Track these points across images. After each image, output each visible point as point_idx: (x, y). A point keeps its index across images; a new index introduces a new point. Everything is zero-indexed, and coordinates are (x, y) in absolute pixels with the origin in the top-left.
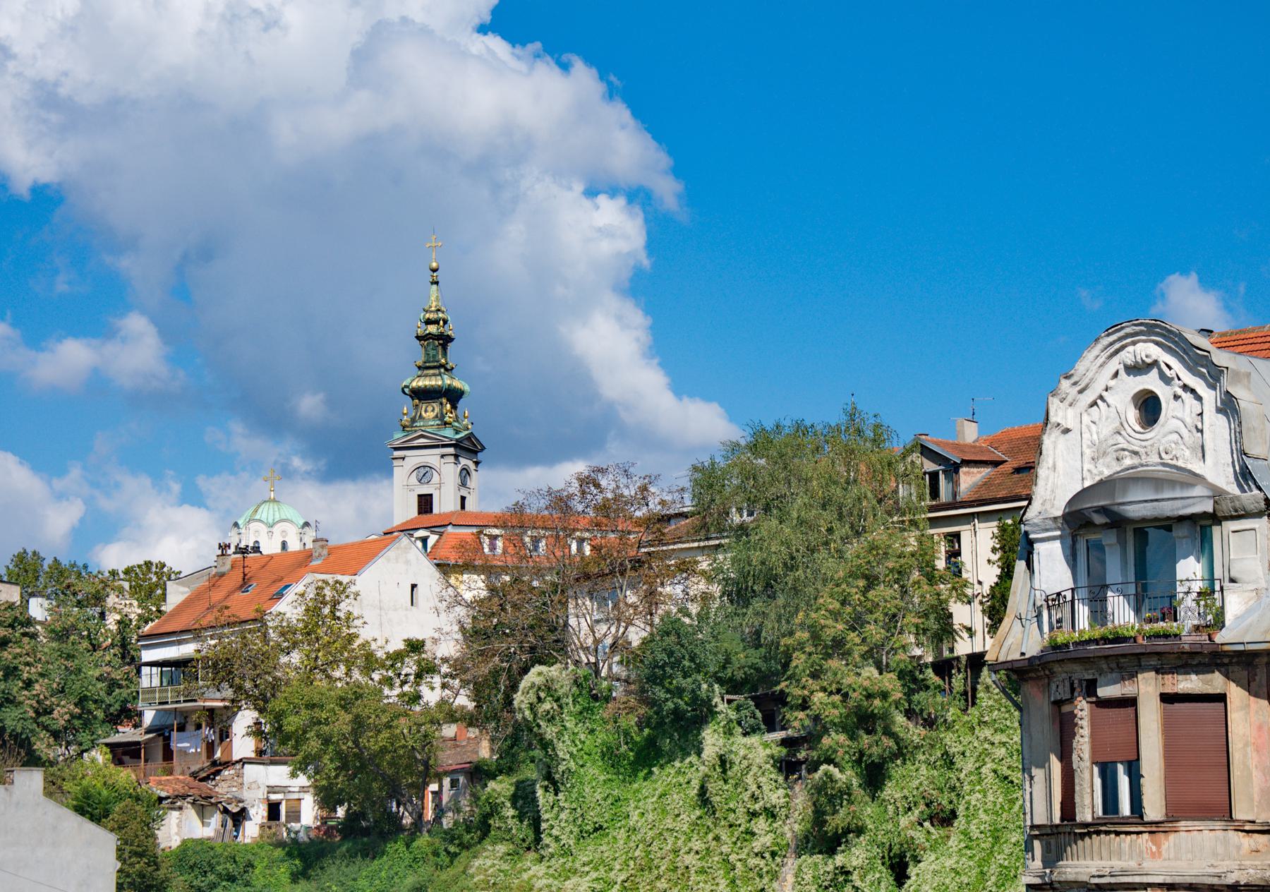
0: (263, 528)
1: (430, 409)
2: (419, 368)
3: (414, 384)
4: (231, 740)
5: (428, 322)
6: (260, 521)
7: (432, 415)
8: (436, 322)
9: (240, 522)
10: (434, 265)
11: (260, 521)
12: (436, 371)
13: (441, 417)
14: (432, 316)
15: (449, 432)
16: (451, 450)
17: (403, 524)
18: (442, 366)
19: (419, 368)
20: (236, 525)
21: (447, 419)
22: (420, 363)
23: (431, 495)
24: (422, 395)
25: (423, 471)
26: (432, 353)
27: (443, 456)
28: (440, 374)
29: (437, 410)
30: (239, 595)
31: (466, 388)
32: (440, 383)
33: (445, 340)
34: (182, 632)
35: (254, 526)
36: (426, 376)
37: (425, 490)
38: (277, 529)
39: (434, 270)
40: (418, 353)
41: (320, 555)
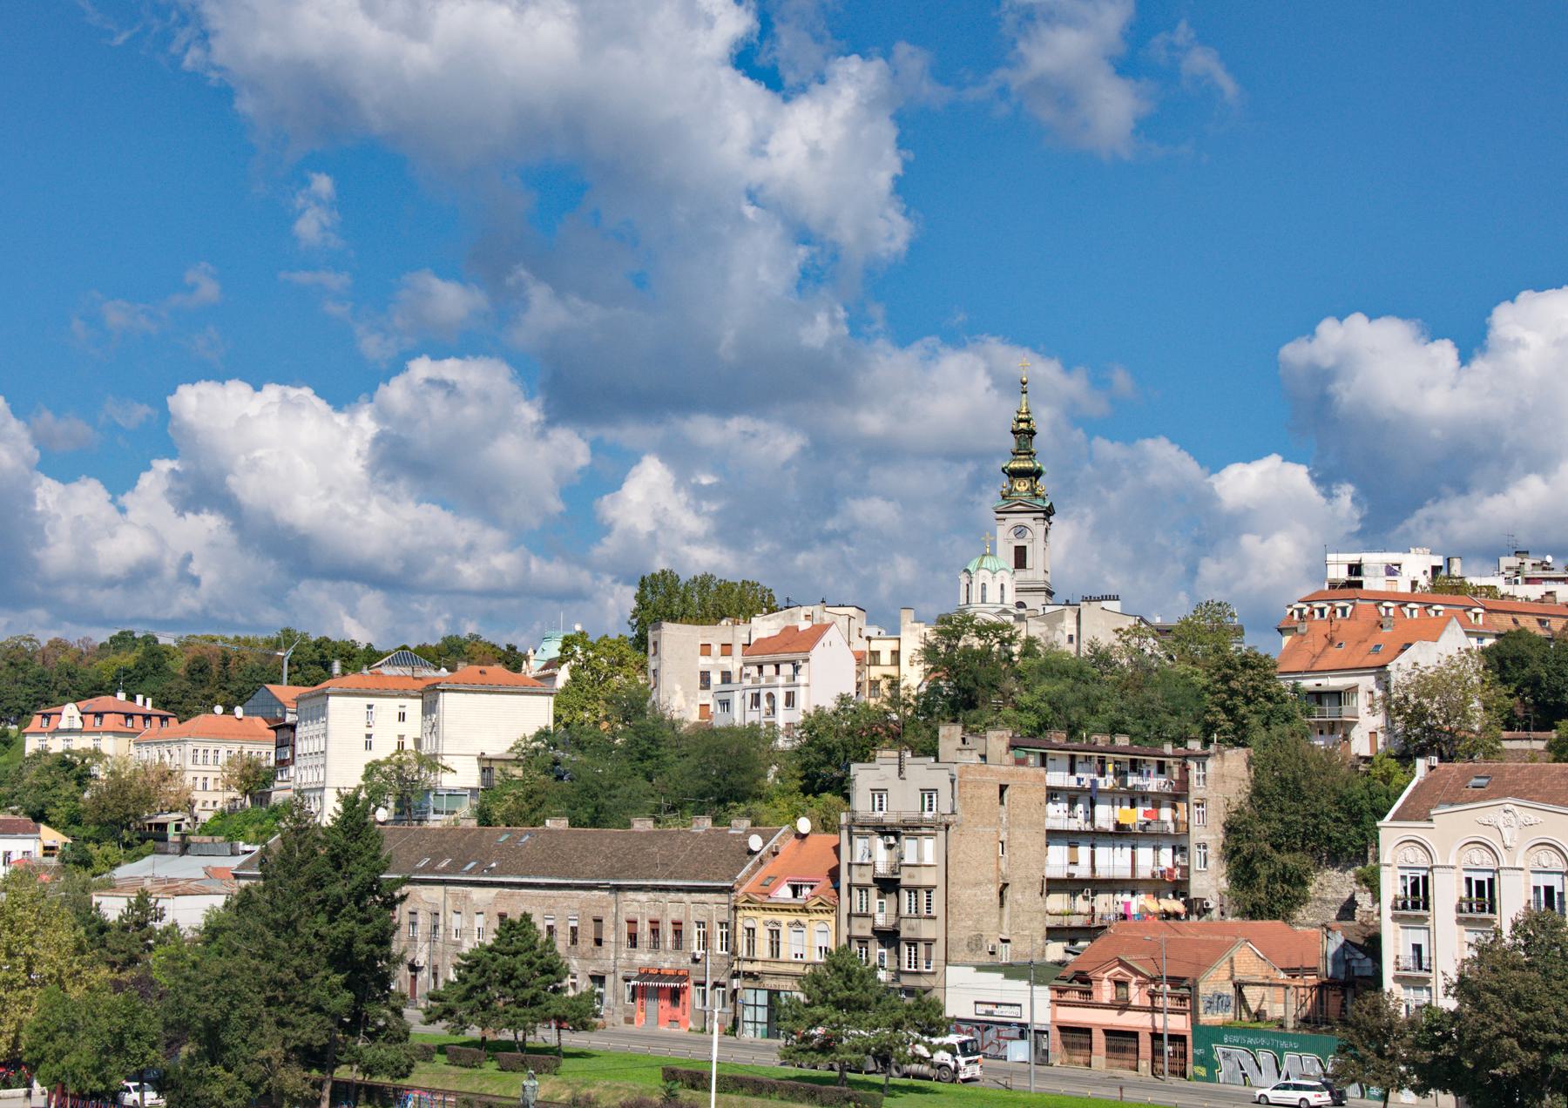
0: (989, 575)
1: (1022, 484)
2: (1014, 454)
3: (1012, 466)
4: (1349, 743)
5: (1021, 421)
6: (986, 569)
7: (1024, 488)
8: (1028, 421)
9: (971, 569)
10: (1024, 379)
11: (986, 569)
12: (1027, 457)
13: (1032, 490)
14: (1023, 417)
15: (1039, 502)
16: (1042, 515)
17: (1310, 596)
18: (1031, 453)
19: (1014, 454)
20: (967, 571)
21: (1038, 492)
22: (1014, 449)
23: (1025, 547)
24: (1015, 474)
25: (1019, 529)
26: (1023, 443)
27: (1035, 519)
28: (1030, 459)
29: (1028, 485)
30: (1331, 649)
31: (1044, 469)
32: (1032, 465)
33: (1032, 433)
34: (1306, 672)
35: (982, 572)
36: (1020, 460)
37: (1021, 543)
38: (998, 575)
39: (1024, 383)
40: (1011, 443)
41: (1389, 627)
